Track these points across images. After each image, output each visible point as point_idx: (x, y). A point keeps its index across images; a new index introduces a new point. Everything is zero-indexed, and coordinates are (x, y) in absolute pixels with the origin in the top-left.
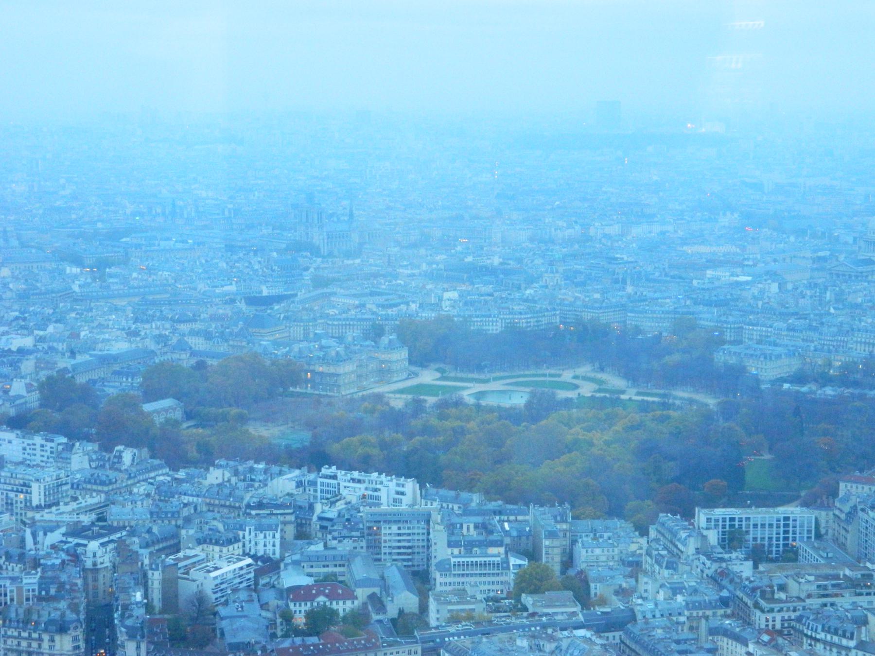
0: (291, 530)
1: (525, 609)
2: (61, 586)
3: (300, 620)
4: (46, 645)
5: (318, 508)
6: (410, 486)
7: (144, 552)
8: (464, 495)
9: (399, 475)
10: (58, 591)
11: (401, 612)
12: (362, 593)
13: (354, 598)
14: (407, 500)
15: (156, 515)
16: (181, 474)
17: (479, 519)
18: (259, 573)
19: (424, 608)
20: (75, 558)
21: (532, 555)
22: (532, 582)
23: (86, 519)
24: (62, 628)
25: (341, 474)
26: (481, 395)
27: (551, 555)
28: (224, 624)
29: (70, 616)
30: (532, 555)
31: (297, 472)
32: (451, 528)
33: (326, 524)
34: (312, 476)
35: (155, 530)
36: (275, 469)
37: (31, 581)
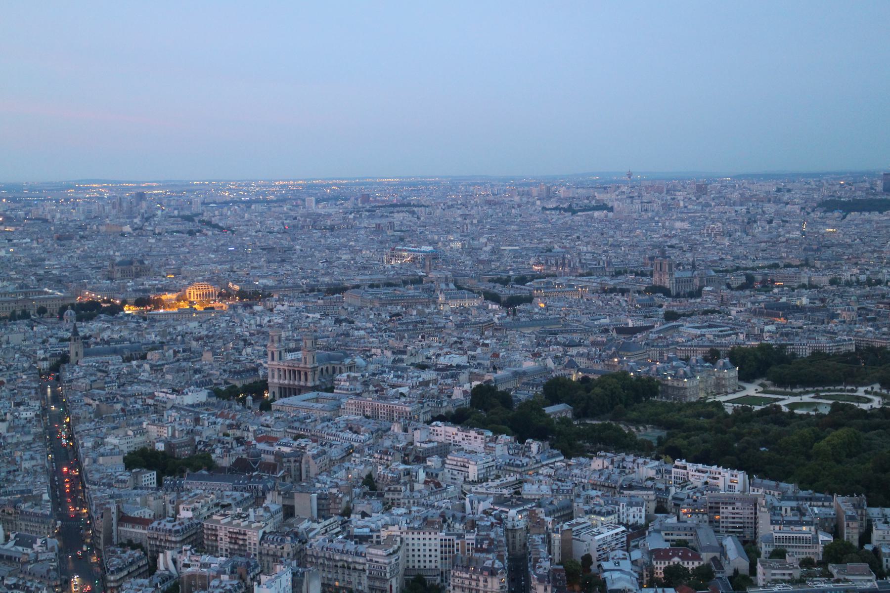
0: (653, 506)
1: (832, 576)
2: (491, 541)
3: (660, 574)
4: (481, 584)
5: (673, 490)
6: (741, 477)
7: (549, 519)
8: (783, 485)
9: (733, 468)
10: (490, 544)
11: (736, 572)
12: (706, 557)
13: (699, 558)
14: (738, 487)
15: (555, 492)
16: (573, 461)
17: (794, 504)
18: (630, 538)
19: (753, 570)
20: (501, 521)
21: (836, 532)
22: (838, 553)
23: (506, 492)
24: (493, 572)
25: (690, 466)
26: (792, 406)
27: (851, 533)
28: (606, 574)
29: (498, 564)
30: (836, 532)
31: (657, 463)
32: (773, 509)
33: (678, 502)
34: (668, 467)
35: (555, 502)
36: (640, 460)
37: (471, 537)
